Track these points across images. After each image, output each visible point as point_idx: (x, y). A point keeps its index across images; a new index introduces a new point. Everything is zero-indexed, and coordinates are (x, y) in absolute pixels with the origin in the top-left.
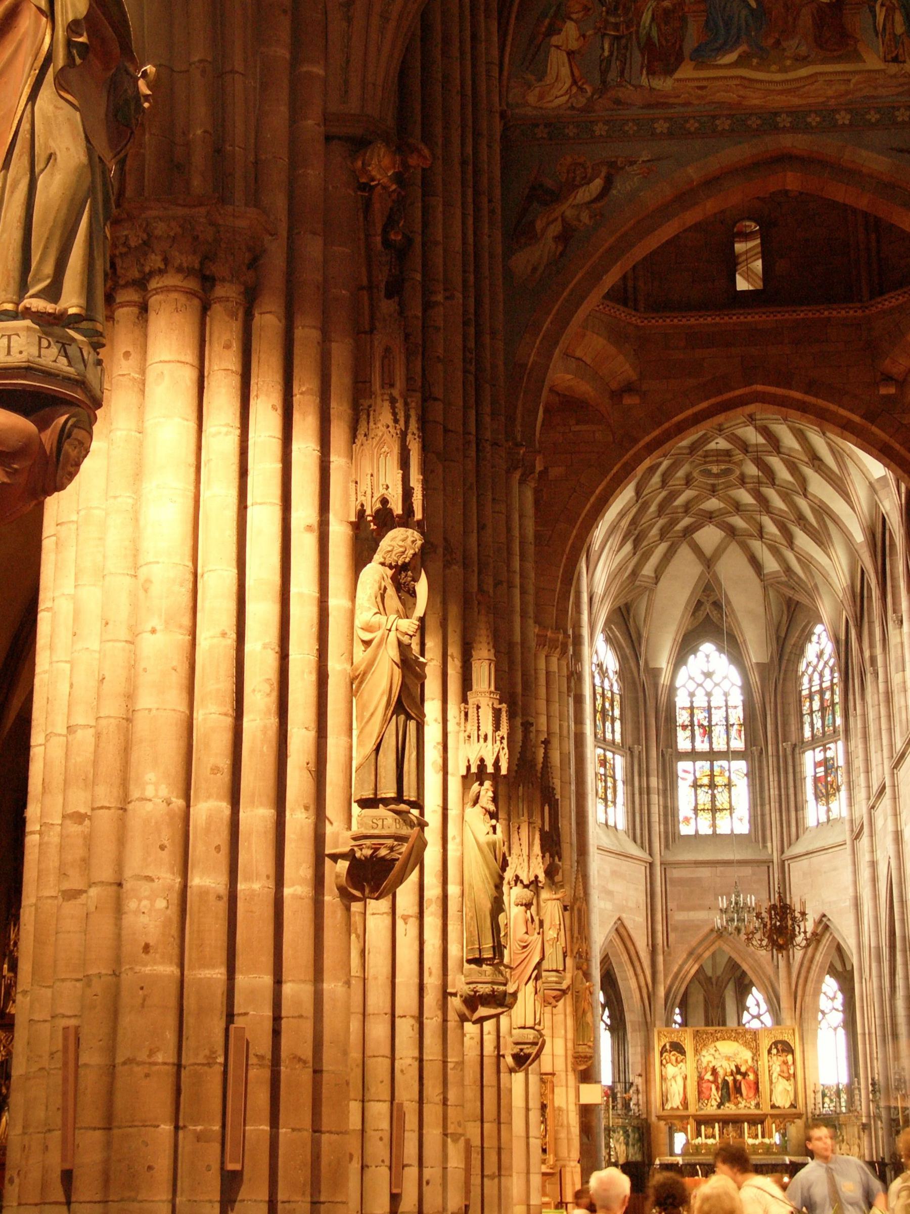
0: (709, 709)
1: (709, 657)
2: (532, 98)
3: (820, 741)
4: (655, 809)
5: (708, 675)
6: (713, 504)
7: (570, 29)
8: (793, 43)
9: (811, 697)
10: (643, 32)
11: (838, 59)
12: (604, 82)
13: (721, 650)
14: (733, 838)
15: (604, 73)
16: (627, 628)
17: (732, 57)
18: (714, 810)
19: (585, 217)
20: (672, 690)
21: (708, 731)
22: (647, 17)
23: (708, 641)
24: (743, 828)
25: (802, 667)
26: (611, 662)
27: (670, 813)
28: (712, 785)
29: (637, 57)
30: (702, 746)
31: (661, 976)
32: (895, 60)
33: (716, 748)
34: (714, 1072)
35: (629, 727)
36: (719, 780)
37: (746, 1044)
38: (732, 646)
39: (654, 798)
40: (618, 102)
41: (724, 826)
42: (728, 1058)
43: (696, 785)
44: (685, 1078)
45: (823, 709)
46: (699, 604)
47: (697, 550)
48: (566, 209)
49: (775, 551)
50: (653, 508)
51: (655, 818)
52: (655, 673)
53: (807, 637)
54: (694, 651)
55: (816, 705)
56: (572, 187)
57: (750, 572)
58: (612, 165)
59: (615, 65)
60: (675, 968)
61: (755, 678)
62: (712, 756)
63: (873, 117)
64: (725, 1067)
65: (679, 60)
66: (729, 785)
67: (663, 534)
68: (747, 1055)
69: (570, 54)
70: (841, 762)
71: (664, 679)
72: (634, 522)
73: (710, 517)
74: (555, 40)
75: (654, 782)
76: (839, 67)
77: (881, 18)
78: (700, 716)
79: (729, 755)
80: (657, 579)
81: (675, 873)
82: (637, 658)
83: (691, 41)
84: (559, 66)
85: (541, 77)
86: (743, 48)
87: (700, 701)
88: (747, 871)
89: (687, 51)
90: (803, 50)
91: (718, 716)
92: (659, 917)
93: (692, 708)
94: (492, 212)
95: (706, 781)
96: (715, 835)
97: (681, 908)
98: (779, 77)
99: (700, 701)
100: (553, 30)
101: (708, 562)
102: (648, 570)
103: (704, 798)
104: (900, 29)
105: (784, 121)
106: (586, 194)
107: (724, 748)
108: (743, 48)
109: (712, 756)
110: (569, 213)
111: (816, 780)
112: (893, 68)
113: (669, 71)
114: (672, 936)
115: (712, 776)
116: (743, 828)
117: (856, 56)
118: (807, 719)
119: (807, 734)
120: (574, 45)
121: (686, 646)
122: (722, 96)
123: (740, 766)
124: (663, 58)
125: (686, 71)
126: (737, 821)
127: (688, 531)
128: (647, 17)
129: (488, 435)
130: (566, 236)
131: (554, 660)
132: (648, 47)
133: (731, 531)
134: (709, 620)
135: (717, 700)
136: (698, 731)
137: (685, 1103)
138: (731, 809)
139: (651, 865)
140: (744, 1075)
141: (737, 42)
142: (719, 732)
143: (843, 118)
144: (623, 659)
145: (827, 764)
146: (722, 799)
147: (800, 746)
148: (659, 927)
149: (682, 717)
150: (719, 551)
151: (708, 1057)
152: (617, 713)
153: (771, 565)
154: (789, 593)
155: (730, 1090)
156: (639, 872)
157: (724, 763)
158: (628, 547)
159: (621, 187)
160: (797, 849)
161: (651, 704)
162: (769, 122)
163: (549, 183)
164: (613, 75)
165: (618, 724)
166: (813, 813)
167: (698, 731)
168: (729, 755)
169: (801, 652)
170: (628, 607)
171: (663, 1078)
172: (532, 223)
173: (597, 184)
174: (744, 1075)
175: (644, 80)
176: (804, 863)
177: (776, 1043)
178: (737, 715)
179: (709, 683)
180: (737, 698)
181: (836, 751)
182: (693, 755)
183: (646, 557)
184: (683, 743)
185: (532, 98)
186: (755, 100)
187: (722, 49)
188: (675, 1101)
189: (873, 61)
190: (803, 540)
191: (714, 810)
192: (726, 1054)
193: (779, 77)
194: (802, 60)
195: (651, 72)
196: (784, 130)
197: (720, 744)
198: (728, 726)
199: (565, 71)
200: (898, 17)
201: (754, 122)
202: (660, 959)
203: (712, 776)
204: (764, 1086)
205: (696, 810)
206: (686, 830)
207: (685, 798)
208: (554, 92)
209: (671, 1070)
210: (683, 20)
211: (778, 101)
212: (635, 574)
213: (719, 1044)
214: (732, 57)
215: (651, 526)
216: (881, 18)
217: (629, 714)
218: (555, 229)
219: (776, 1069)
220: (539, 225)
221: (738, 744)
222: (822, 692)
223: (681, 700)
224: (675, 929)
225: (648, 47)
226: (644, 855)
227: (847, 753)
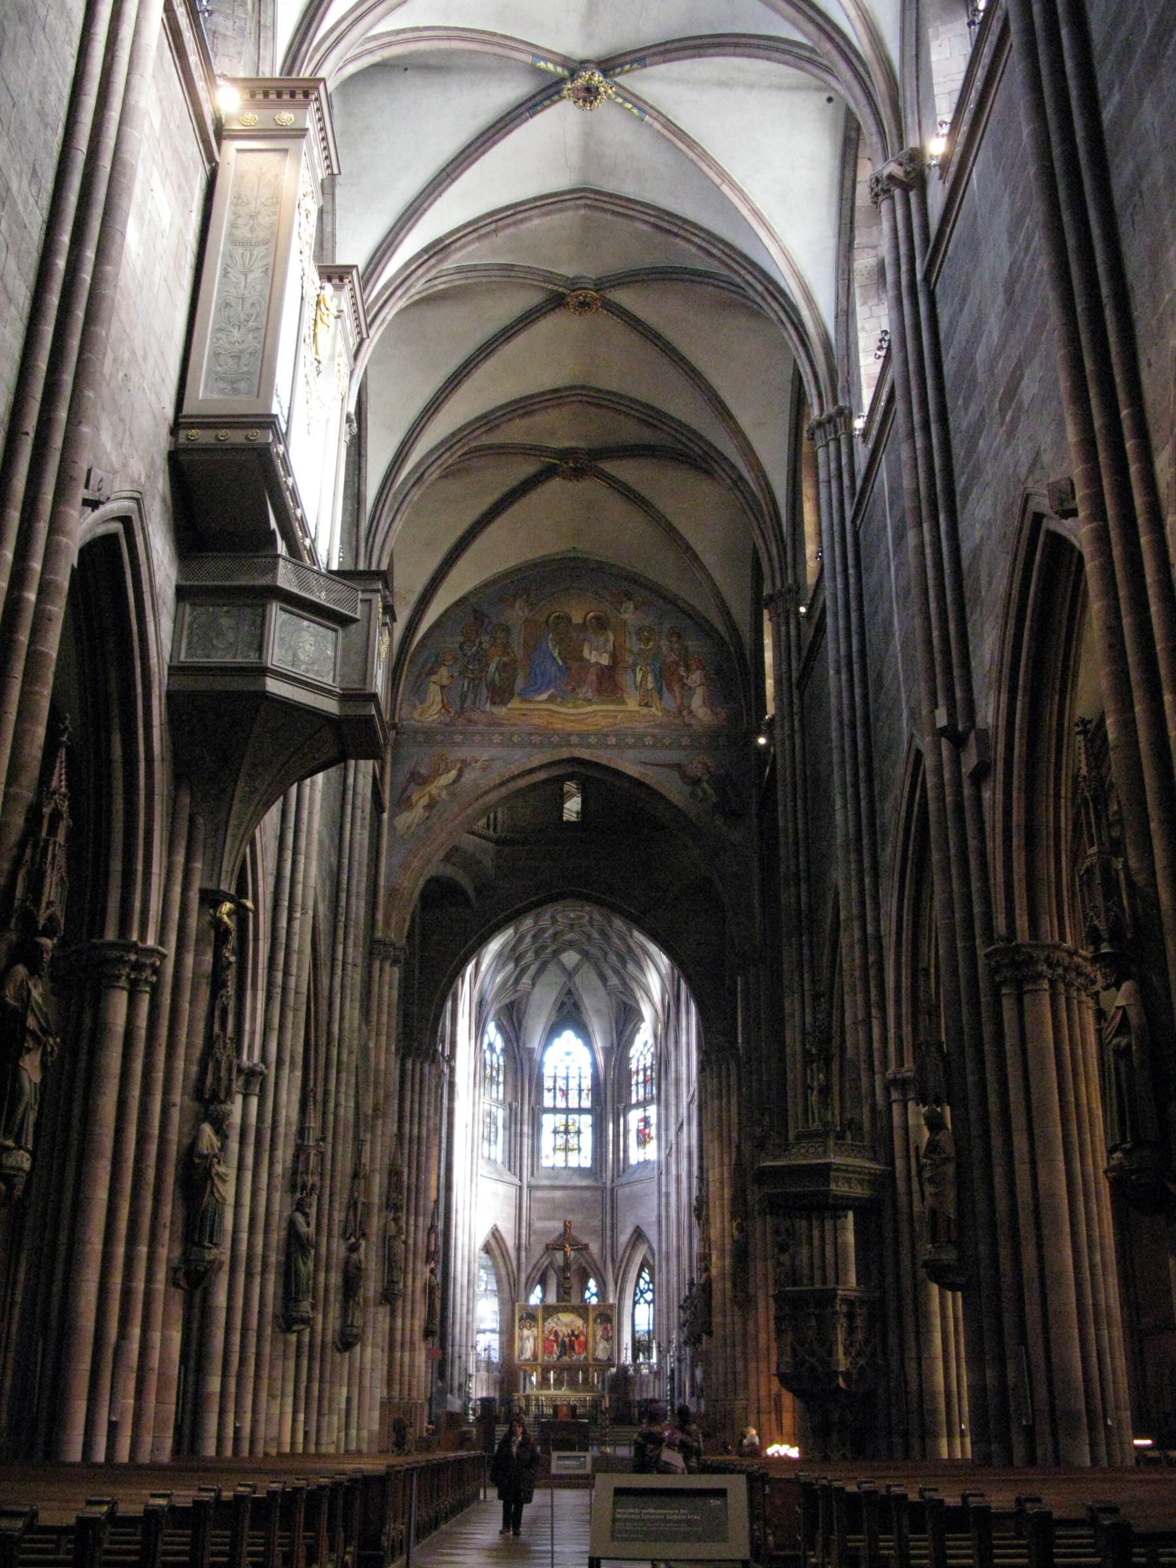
0: (567, 1078)
1: (568, 1039)
2: (416, 715)
3: (643, 1104)
4: (525, 1148)
5: (568, 1054)
6: (569, 936)
7: (444, 671)
8: (584, 690)
9: (637, 1072)
10: (490, 675)
11: (612, 702)
12: (462, 707)
13: (578, 1035)
14: (579, 1170)
15: (463, 701)
16: (513, 1019)
17: (544, 696)
18: (566, 1149)
19: (444, 794)
20: (541, 1064)
21: (565, 1094)
22: (493, 667)
23: (569, 1027)
24: (587, 1163)
25: (633, 1052)
26: (499, 1043)
27: (535, 1151)
28: (567, 1132)
29: (485, 691)
30: (561, 1104)
31: (523, 1266)
32: (646, 705)
33: (571, 1106)
34: (556, 1334)
35: (509, 1088)
36: (572, 1129)
37: (580, 1316)
38: (585, 1034)
39: (525, 1140)
40: (470, 721)
41: (573, 1163)
42: (566, 1325)
43: (555, 1132)
44: (535, 1339)
45: (645, 1082)
46: (563, 1004)
47: (563, 968)
48: (433, 789)
49: (616, 971)
50: (528, 939)
51: (525, 1154)
52: (531, 1051)
53: (636, 1030)
54: (559, 1035)
55: (641, 1078)
56: (436, 774)
57: (599, 983)
58: (463, 761)
59: (471, 696)
60: (533, 1261)
61: (600, 1059)
62: (567, 1111)
63: (630, 740)
64: (564, 1331)
65: (512, 695)
66: (579, 1132)
67: (537, 954)
68: (579, 1323)
69: (443, 687)
70: (653, 1120)
71: (537, 1056)
72: (514, 949)
73: (571, 944)
74: (434, 678)
75: (525, 1128)
76: (611, 707)
77: (639, 677)
78: (561, 1083)
79: (580, 1111)
80: (533, 985)
81: (538, 1194)
82: (518, 1039)
83: (520, 683)
84: (434, 694)
85: (422, 701)
86: (551, 691)
87: (562, 1073)
88: (587, 1194)
89: (517, 690)
90: (590, 695)
91: (573, 1084)
92: (524, 1224)
93: (555, 1078)
94: (363, 819)
95: (562, 1129)
96: (566, 1168)
97: (540, 1219)
98: (572, 711)
99: (562, 1073)
100: (431, 672)
101: (570, 974)
102: (526, 980)
103: (560, 1140)
104: (650, 686)
105: (574, 739)
106: (445, 780)
107: (576, 1106)
108: (551, 691)
109: (567, 1111)
110: (434, 792)
111: (639, 1131)
112: (645, 710)
113: (504, 703)
114: (533, 1238)
115: (567, 1126)
116: (587, 1163)
117: (622, 702)
118: (634, 1088)
119: (634, 1100)
120: (445, 682)
121: (553, 1032)
122: (536, 721)
123: (587, 1120)
124: (501, 694)
125: (515, 704)
126: (585, 1159)
127: (556, 953)
128: (493, 667)
129: (350, 960)
130: (429, 807)
131: (426, 1066)
132: (491, 686)
133: (585, 954)
134: (569, 1015)
135: (573, 1073)
136: (559, 1094)
137: (535, 1356)
138: (579, 1149)
139: (521, 1188)
140: (577, 1337)
141: (547, 688)
142: (573, 1095)
143: (612, 740)
144: (507, 1040)
145: (646, 1121)
146: (573, 1141)
147: (629, 1107)
148: (524, 1231)
149: (548, 1083)
150: (577, 968)
151: (551, 1324)
152: (501, 1079)
153: (614, 981)
154: (625, 999)
155: (567, 1347)
156: (513, 1191)
157: (575, 1116)
158: (511, 966)
159: (469, 776)
160: (624, 1180)
161: (526, 1072)
162: (565, 739)
163: (423, 771)
164: (468, 703)
165: (501, 1087)
166: (636, 1155)
167: (559, 1094)
168: (580, 1111)
169: (630, 1042)
170: (512, 1003)
171: (521, 1338)
172: (409, 797)
173: (453, 773)
174: (577, 1337)
175: (488, 707)
176: (627, 1189)
177: (600, 1315)
178: (587, 1083)
179: (568, 1060)
180: (588, 1072)
181: (652, 1111)
182: (554, 1110)
183: (523, 971)
184: (548, 1101)
185: (416, 715)
186: (558, 726)
187: (539, 691)
188: (528, 1354)
189: (632, 704)
190: (631, 967)
191: (566, 1149)
192: (566, 1322)
193: (572, 711)
194: (589, 702)
195: (493, 703)
196: (576, 746)
197: (573, 1104)
198: (580, 1091)
199: (438, 698)
200: (650, 678)
201: (555, 739)
202: (523, 1254)
203: (567, 1126)
204: (590, 1345)
205: (555, 1149)
206: (546, 1163)
207: (547, 1140)
208: (431, 712)
209: (526, 1332)
210: (515, 669)
211: (569, 727)
212: (517, 981)
213: (561, 1315)
214: (544, 696)
215: (526, 952)
216: (639, 677)
217: (510, 1080)
218: (425, 801)
219: (599, 1333)
220: (414, 798)
221: (587, 1103)
222: (645, 1070)
223: (548, 1071)
224: (535, 1233)
225: (491, 686)
226: (517, 1181)
227: (659, 1114)
